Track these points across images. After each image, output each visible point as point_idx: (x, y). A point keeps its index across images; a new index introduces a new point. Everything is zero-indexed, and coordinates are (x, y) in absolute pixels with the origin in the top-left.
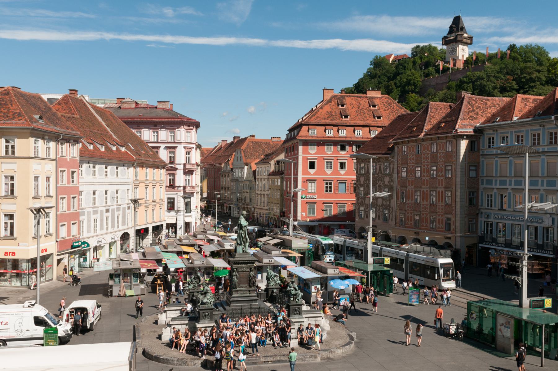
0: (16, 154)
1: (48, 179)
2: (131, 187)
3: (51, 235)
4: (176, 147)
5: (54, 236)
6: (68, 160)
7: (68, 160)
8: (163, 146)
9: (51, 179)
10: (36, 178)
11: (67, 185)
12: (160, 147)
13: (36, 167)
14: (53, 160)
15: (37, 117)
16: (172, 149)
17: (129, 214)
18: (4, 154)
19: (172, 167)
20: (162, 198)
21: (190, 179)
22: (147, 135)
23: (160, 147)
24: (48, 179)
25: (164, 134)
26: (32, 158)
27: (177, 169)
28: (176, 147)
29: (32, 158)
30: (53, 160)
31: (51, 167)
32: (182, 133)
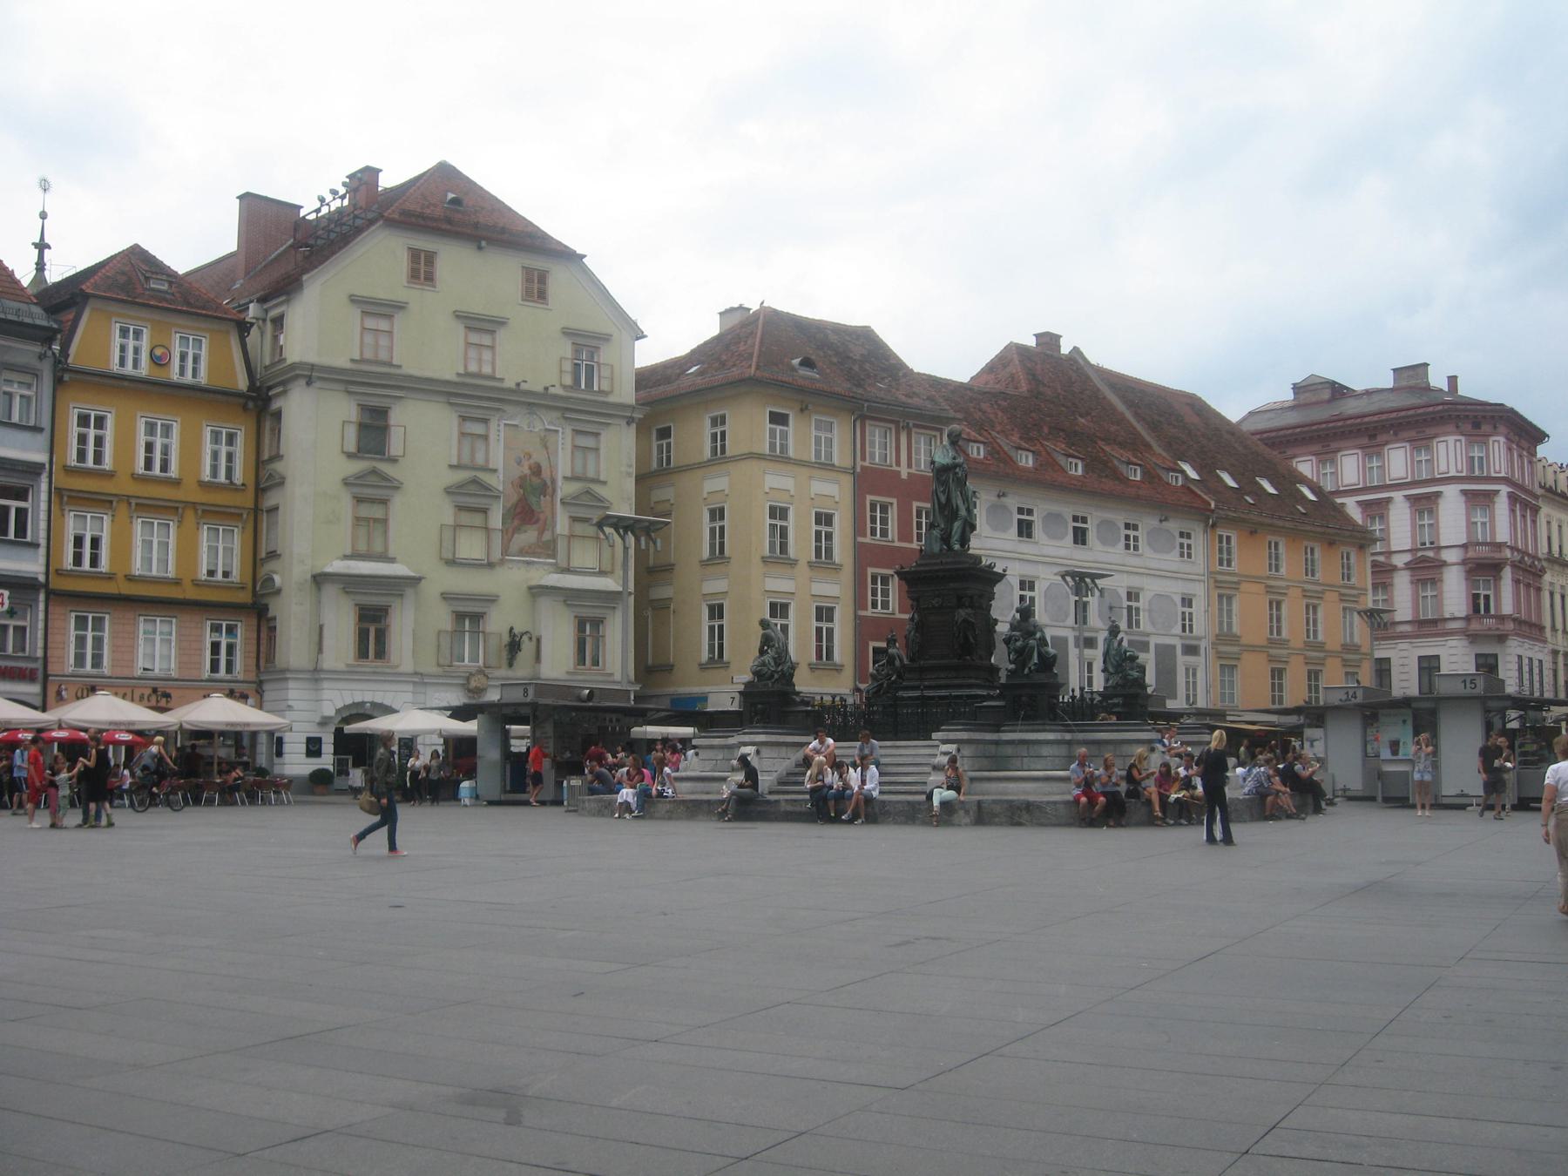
0: (728, 453)
1: (824, 519)
2: (1199, 591)
3: (838, 669)
4: (1438, 495)
5: (849, 672)
6: (904, 476)
7: (904, 476)
8: (1398, 496)
9: (836, 520)
10: (778, 513)
11: (897, 544)
12: (1389, 500)
13: (778, 482)
14: (842, 470)
15: (796, 362)
16: (1424, 504)
17: (1191, 672)
18: (707, 453)
19: (1425, 559)
20: (1357, 640)
21: (1491, 593)
22: (1350, 468)
23: (1389, 500)
24: (824, 519)
25: (1398, 461)
26: (760, 457)
27: (1444, 564)
28: (1438, 495)
29: (760, 457)
30: (842, 470)
31: (834, 492)
32: (1449, 453)
